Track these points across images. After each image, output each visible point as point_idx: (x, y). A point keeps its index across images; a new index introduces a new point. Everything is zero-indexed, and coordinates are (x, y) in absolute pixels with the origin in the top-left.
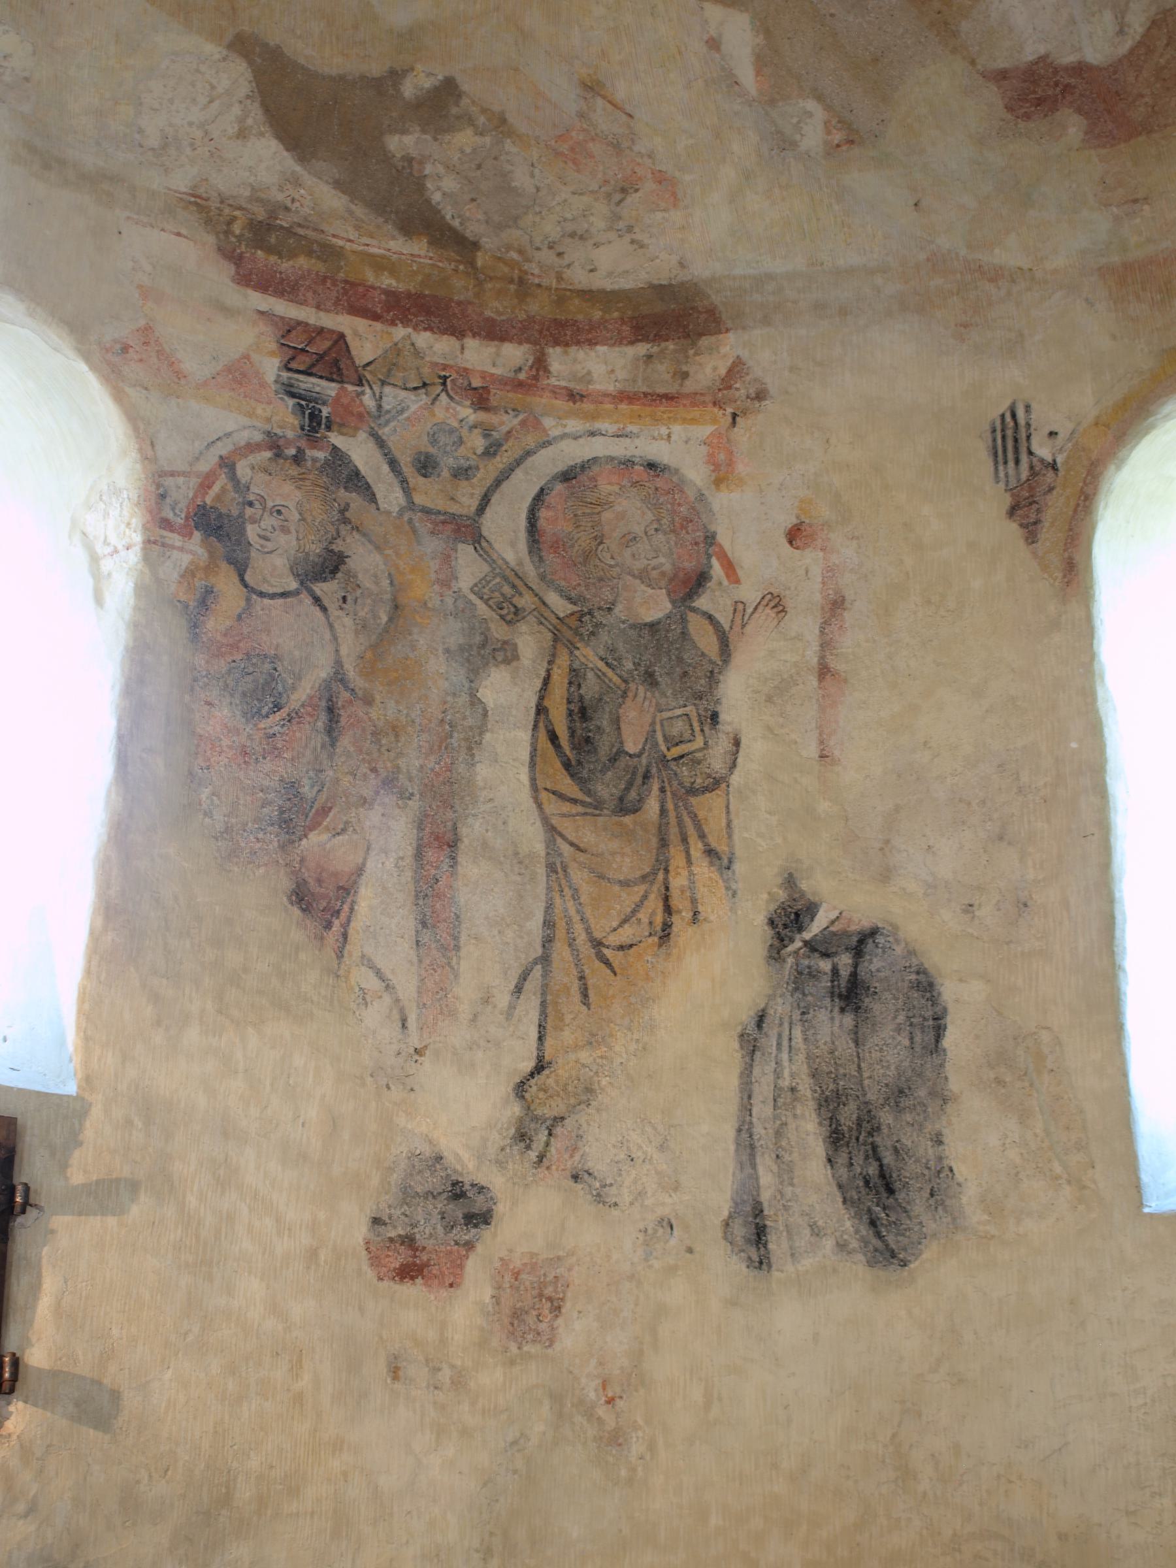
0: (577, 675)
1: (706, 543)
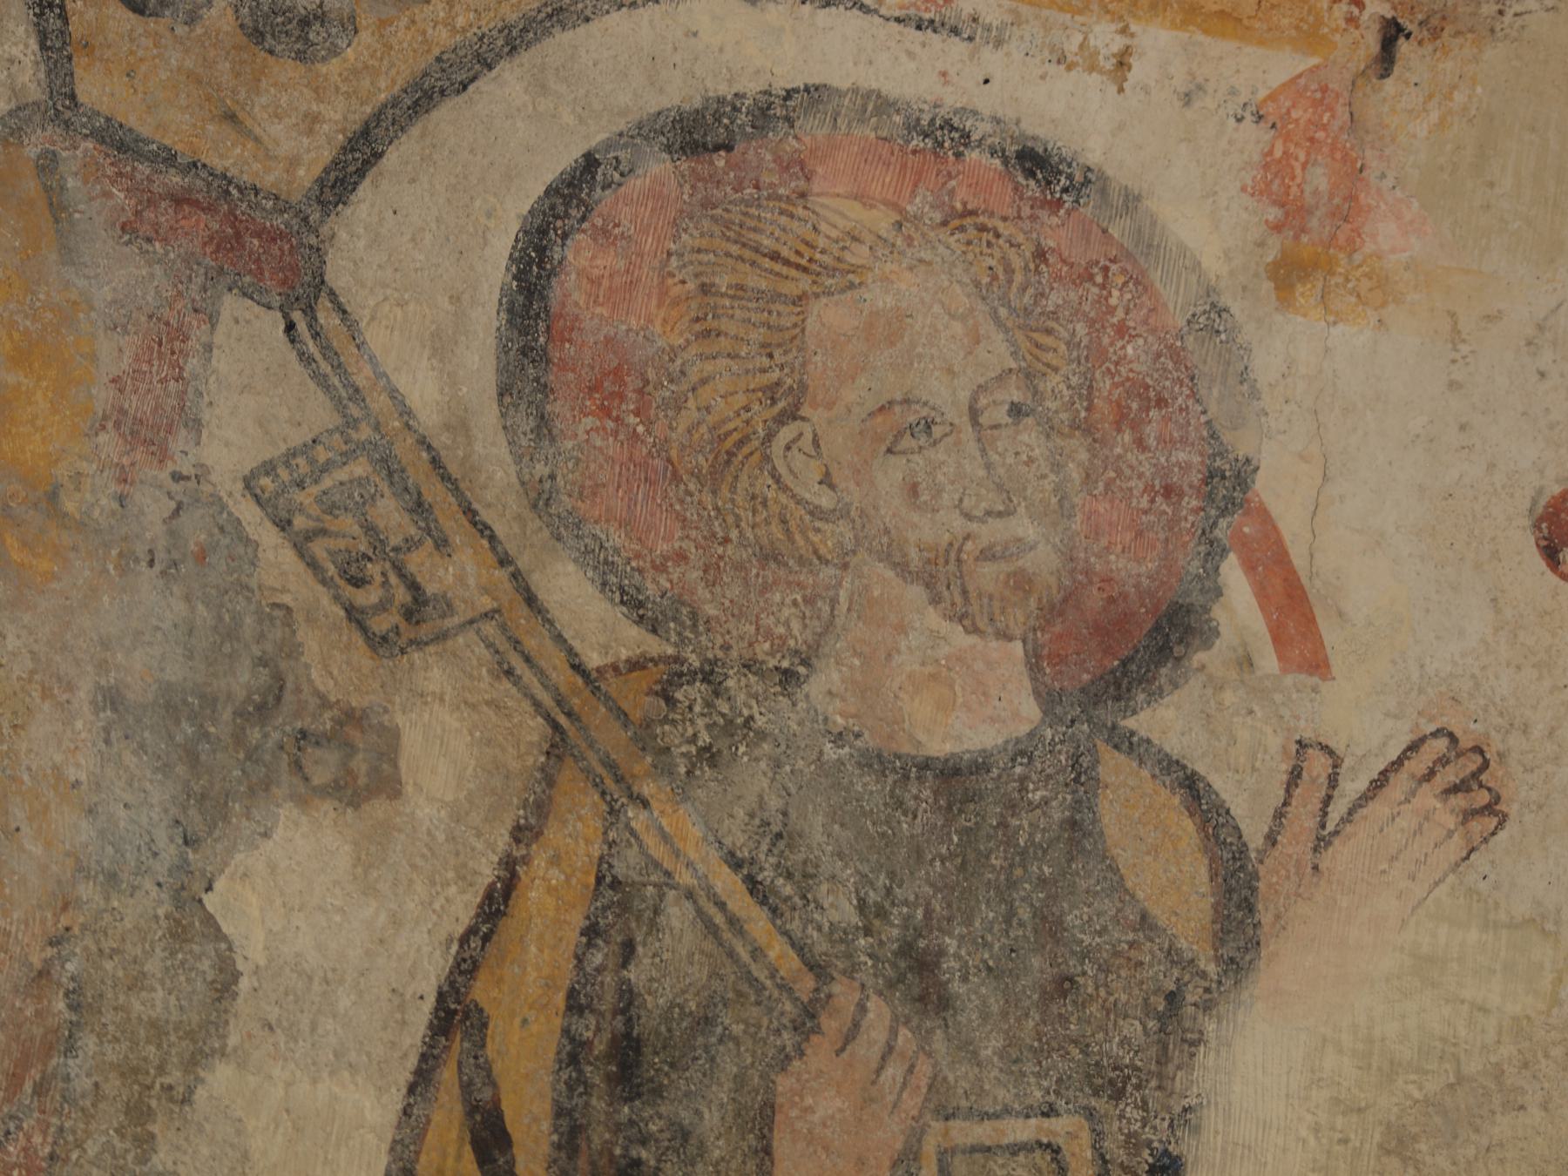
0: (624, 907)
1: (1210, 497)
